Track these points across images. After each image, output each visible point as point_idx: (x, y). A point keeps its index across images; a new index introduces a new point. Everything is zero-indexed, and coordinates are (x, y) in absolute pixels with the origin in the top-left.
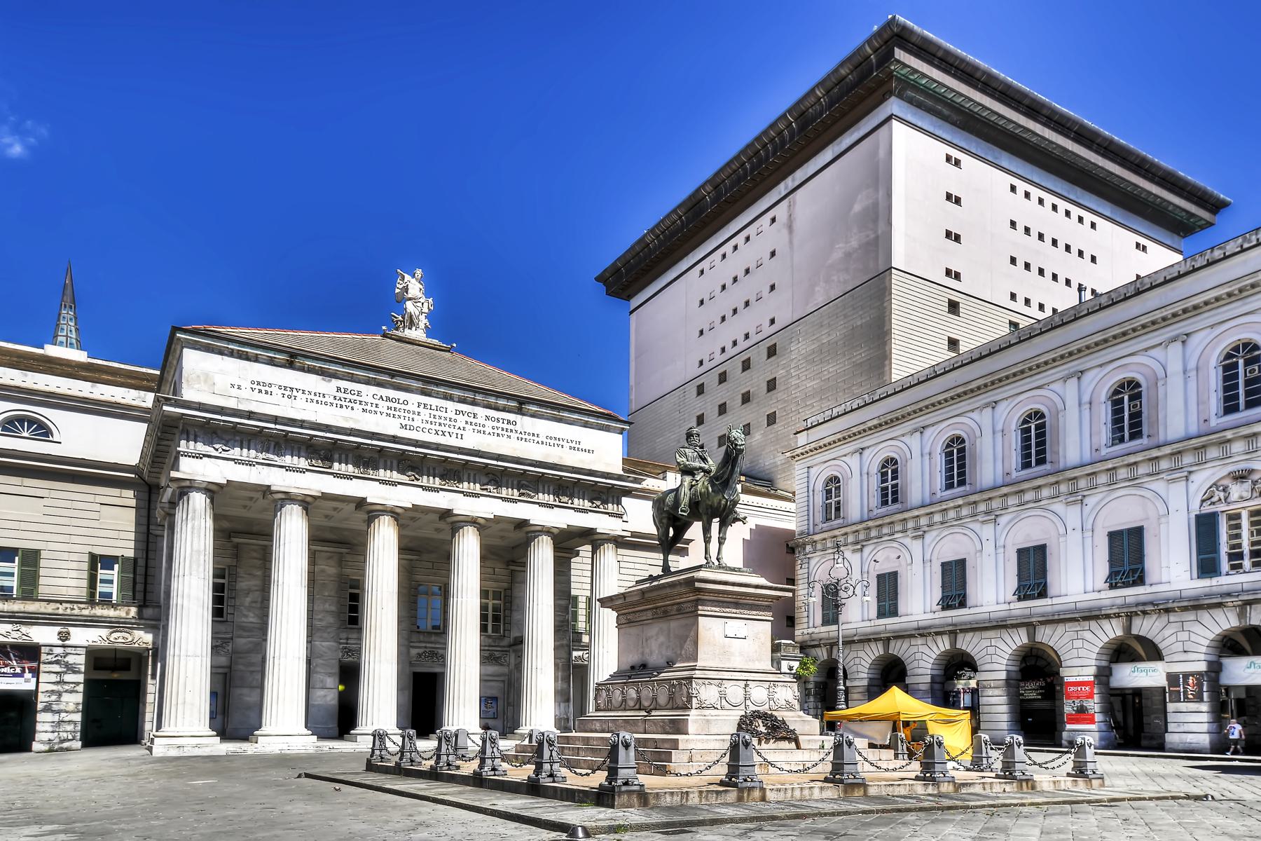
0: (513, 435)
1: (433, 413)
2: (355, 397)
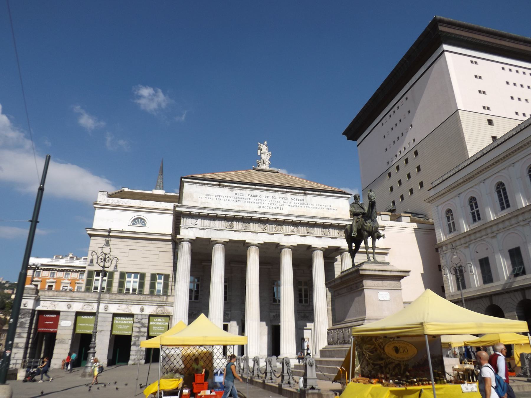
0: (303, 206)
1: (271, 199)
2: (242, 197)
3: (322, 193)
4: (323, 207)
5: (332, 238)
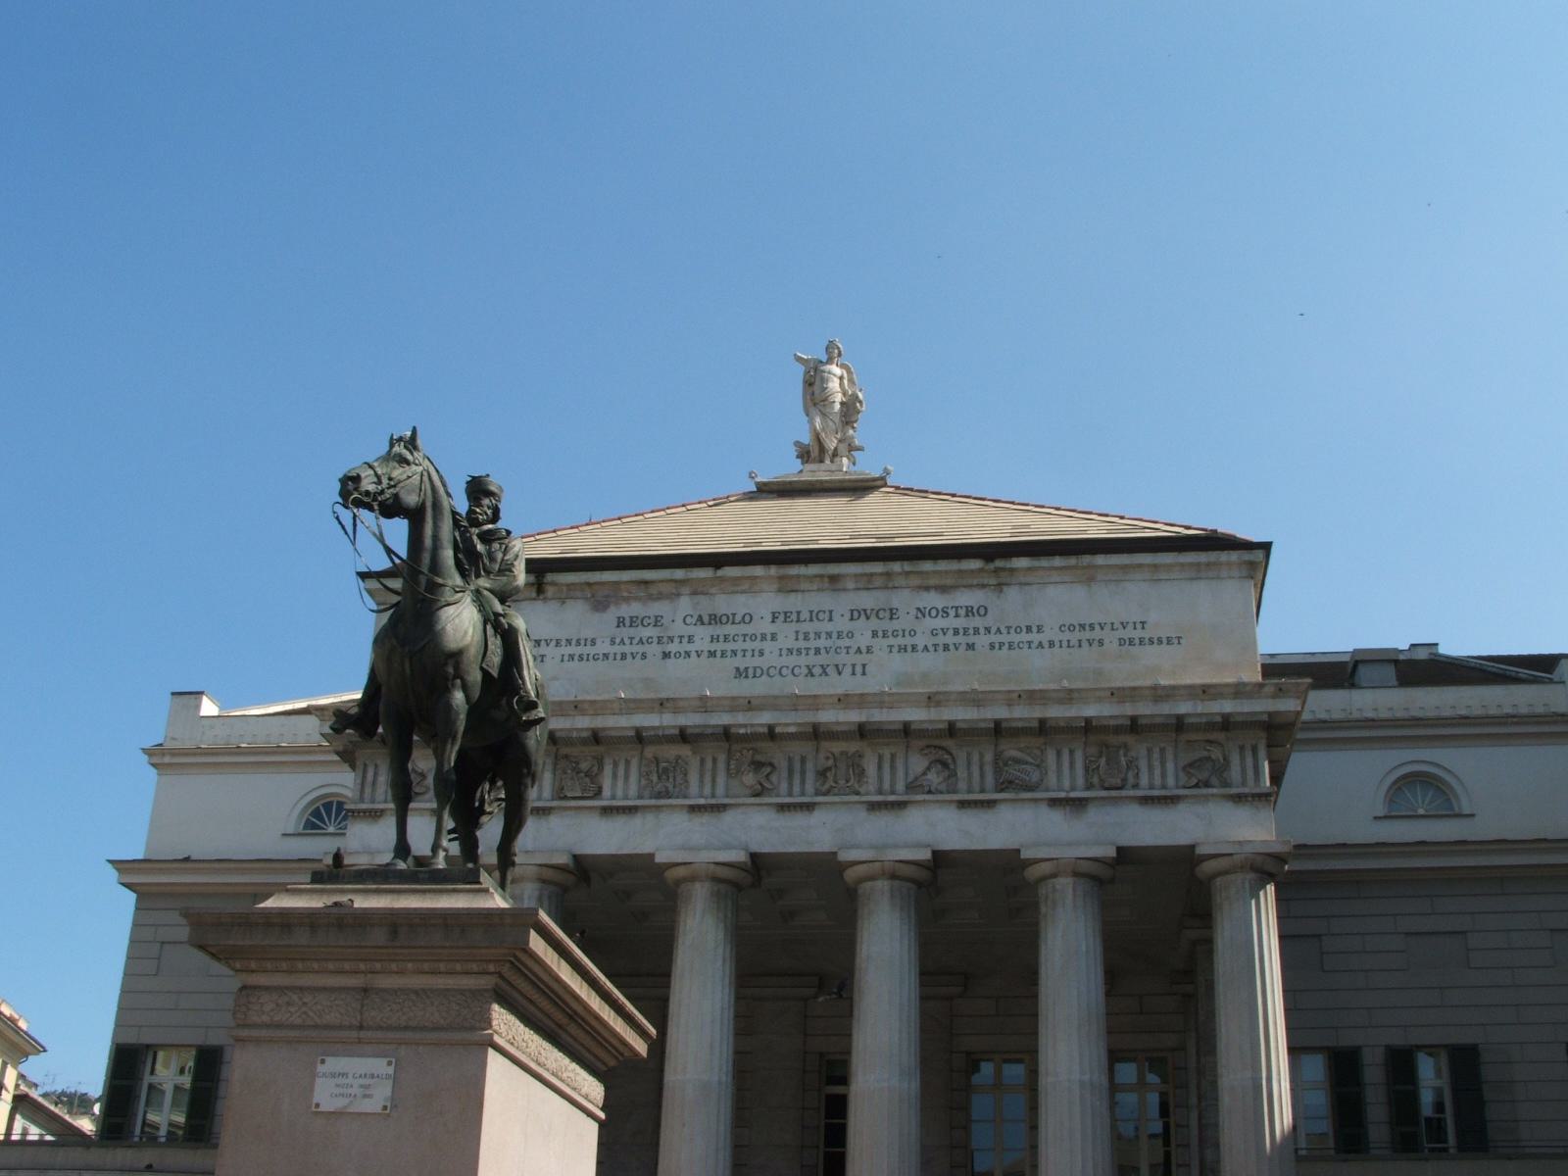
0: (982, 641)
1: (806, 627)
3: (1086, 559)
4: (1097, 634)
5: (1146, 801)
